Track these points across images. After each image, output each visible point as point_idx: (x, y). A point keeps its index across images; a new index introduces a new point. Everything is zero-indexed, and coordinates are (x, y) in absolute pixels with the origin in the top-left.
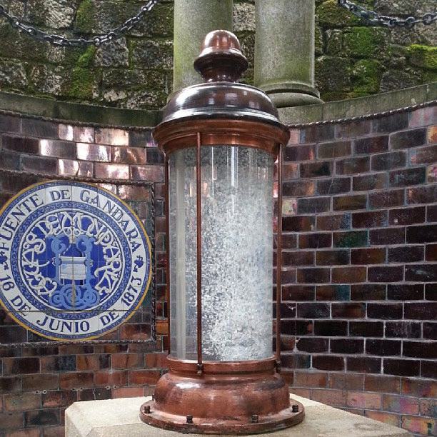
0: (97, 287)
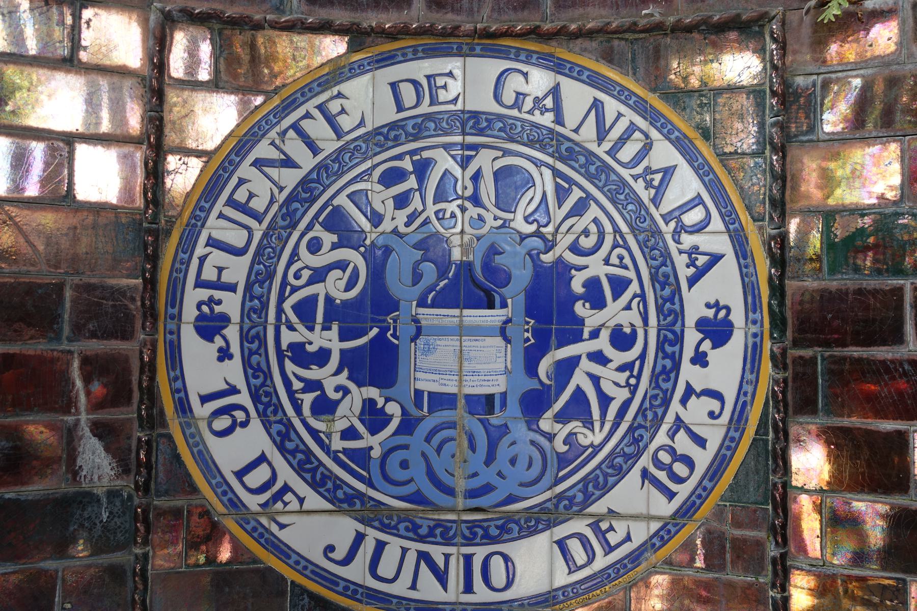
0: (545, 424)
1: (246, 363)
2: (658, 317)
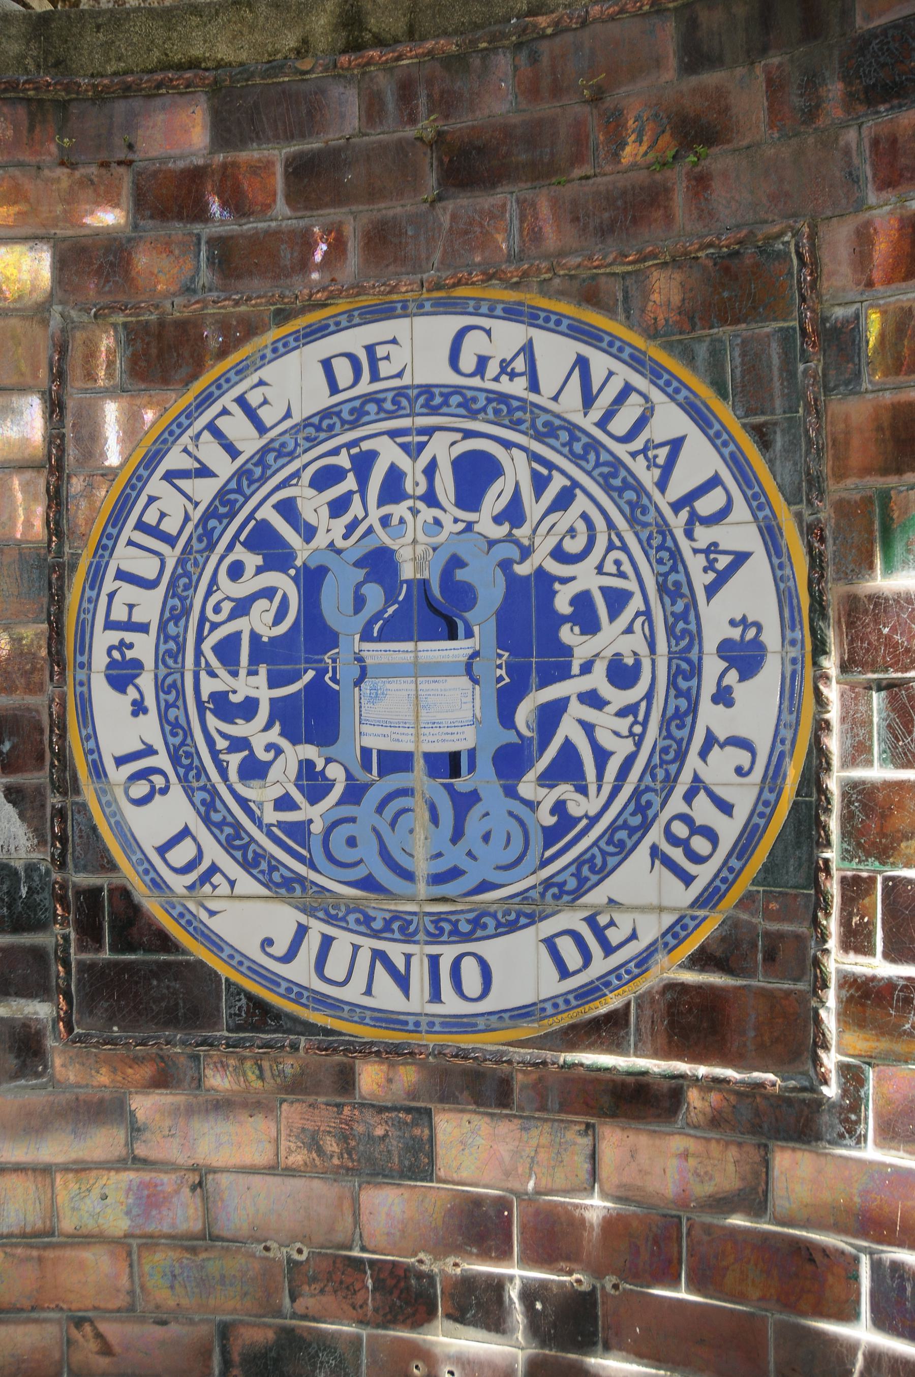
0: (527, 788)
1: (163, 718)
2: (668, 641)
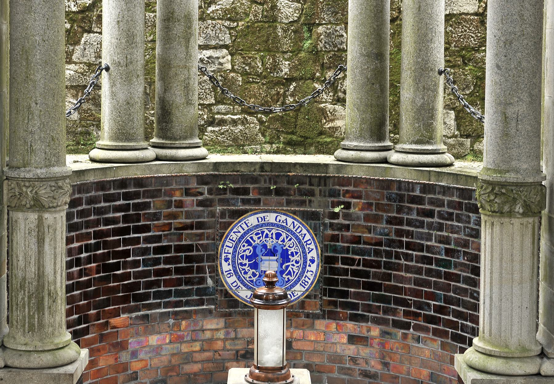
0: (284, 276)
